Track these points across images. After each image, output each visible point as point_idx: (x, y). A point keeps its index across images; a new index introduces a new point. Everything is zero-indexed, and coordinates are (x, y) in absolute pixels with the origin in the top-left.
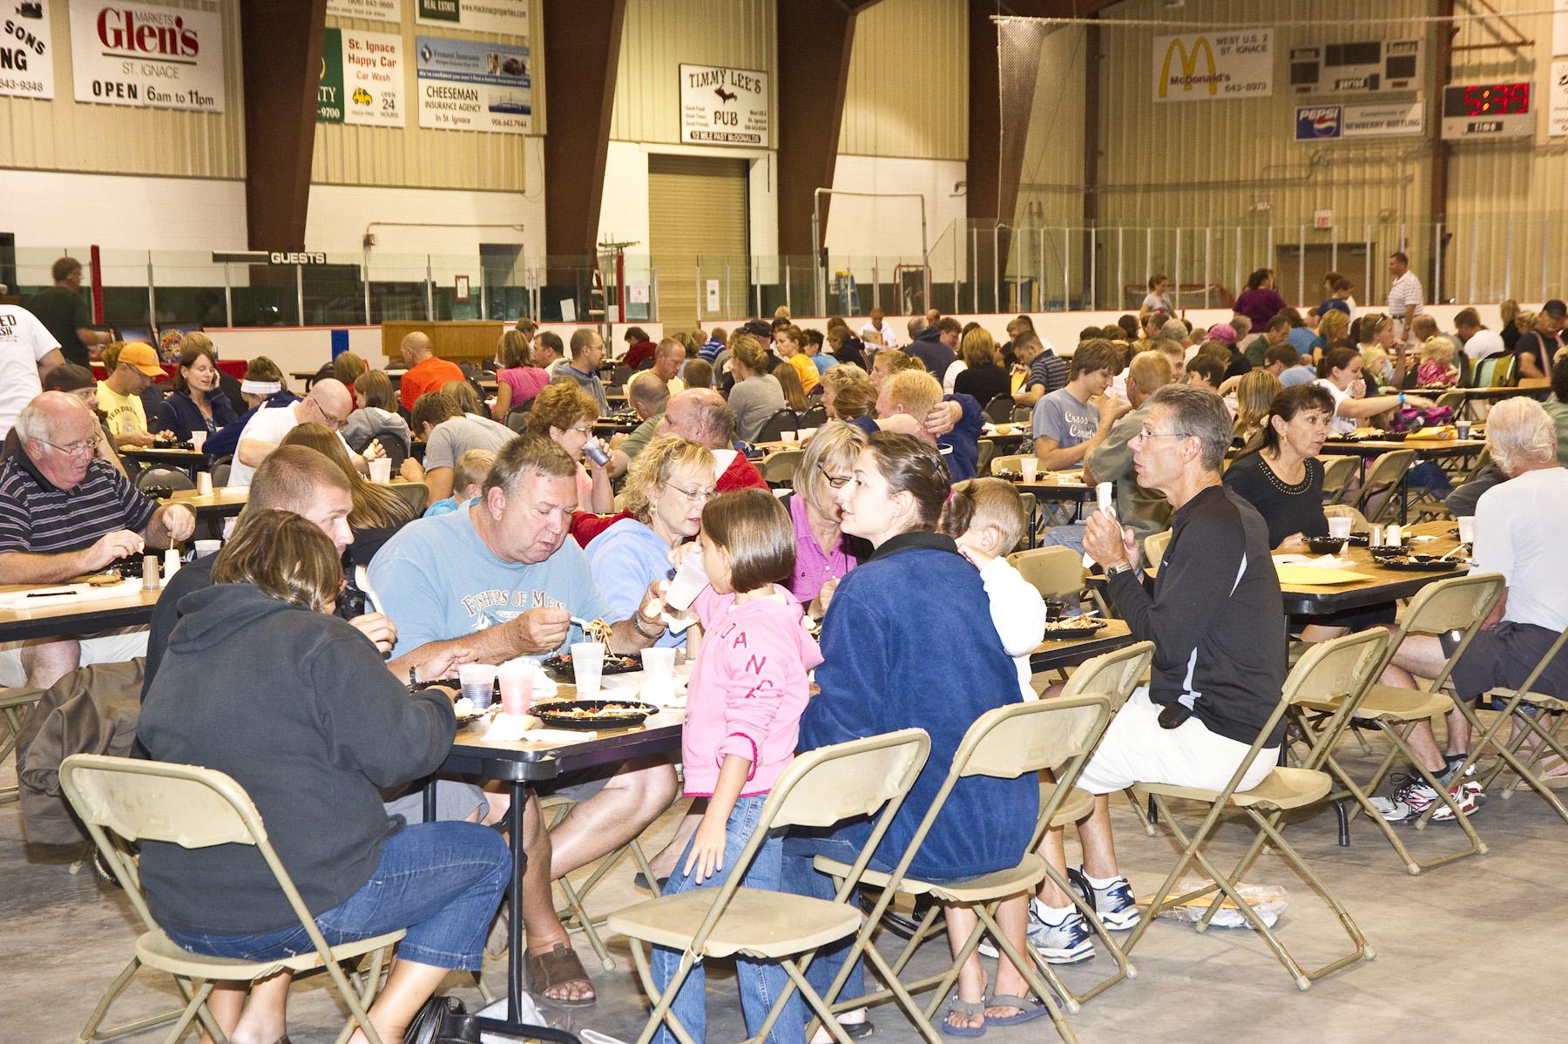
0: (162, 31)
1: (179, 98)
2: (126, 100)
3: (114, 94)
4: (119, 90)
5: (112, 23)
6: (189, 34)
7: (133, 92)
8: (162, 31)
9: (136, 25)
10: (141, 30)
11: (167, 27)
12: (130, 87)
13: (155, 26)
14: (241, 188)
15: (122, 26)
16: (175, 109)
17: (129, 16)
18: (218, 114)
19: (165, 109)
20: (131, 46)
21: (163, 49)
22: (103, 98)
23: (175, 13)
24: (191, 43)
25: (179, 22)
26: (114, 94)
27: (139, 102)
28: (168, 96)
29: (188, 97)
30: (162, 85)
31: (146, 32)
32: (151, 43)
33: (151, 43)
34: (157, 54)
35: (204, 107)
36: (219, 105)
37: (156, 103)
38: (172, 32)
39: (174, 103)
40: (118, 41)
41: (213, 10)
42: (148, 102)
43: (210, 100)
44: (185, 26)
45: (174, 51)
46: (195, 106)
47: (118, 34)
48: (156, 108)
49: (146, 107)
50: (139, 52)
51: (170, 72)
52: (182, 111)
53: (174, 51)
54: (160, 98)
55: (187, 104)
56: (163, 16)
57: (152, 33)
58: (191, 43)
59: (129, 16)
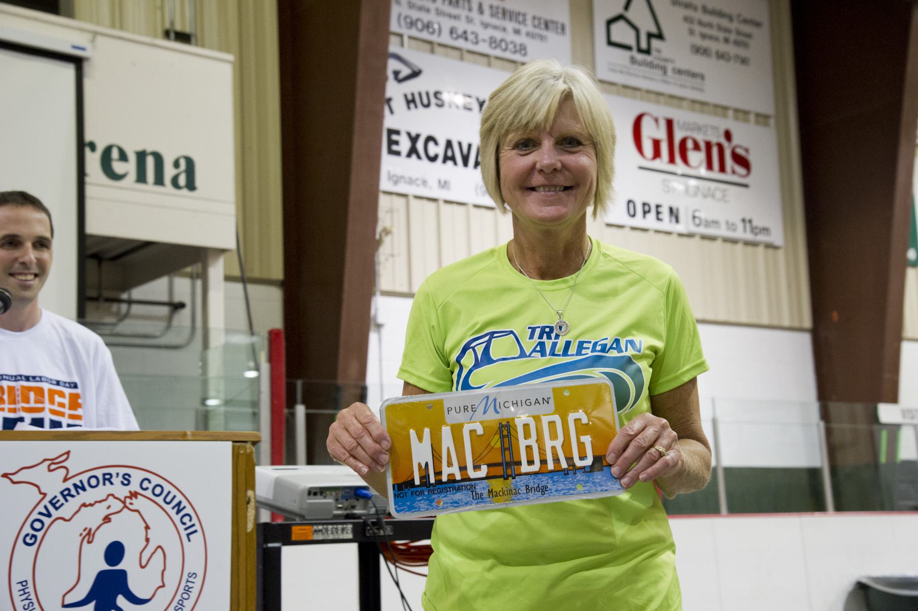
0: (709, 145)
1: (731, 226)
2: (666, 224)
3: (652, 216)
4: (658, 213)
5: (650, 131)
6: (740, 151)
7: (674, 213)
8: (709, 145)
9: (678, 136)
10: (683, 142)
11: (714, 140)
12: (671, 210)
13: (701, 139)
14: (806, 340)
15: (662, 135)
16: (726, 240)
17: (670, 123)
18: (776, 248)
19: (712, 238)
20: (672, 160)
21: (710, 166)
22: (638, 221)
23: (724, 124)
24: (742, 161)
25: (728, 135)
26: (652, 216)
27: (681, 228)
28: (716, 223)
29: (740, 225)
30: (709, 210)
31: (690, 144)
32: (696, 158)
33: (696, 158)
34: (703, 171)
35: (761, 238)
36: (777, 237)
37: (702, 230)
38: (721, 148)
39: (723, 232)
40: (657, 154)
41: (766, 124)
42: (693, 229)
43: (766, 230)
44: (736, 141)
45: (722, 169)
46: (749, 236)
47: (656, 144)
48: (704, 237)
49: (690, 235)
50: (680, 167)
51: (719, 195)
52: (734, 241)
53: (722, 169)
54: (708, 224)
55: (739, 234)
56: (709, 128)
57: (697, 147)
58: (742, 161)
59: (670, 123)
